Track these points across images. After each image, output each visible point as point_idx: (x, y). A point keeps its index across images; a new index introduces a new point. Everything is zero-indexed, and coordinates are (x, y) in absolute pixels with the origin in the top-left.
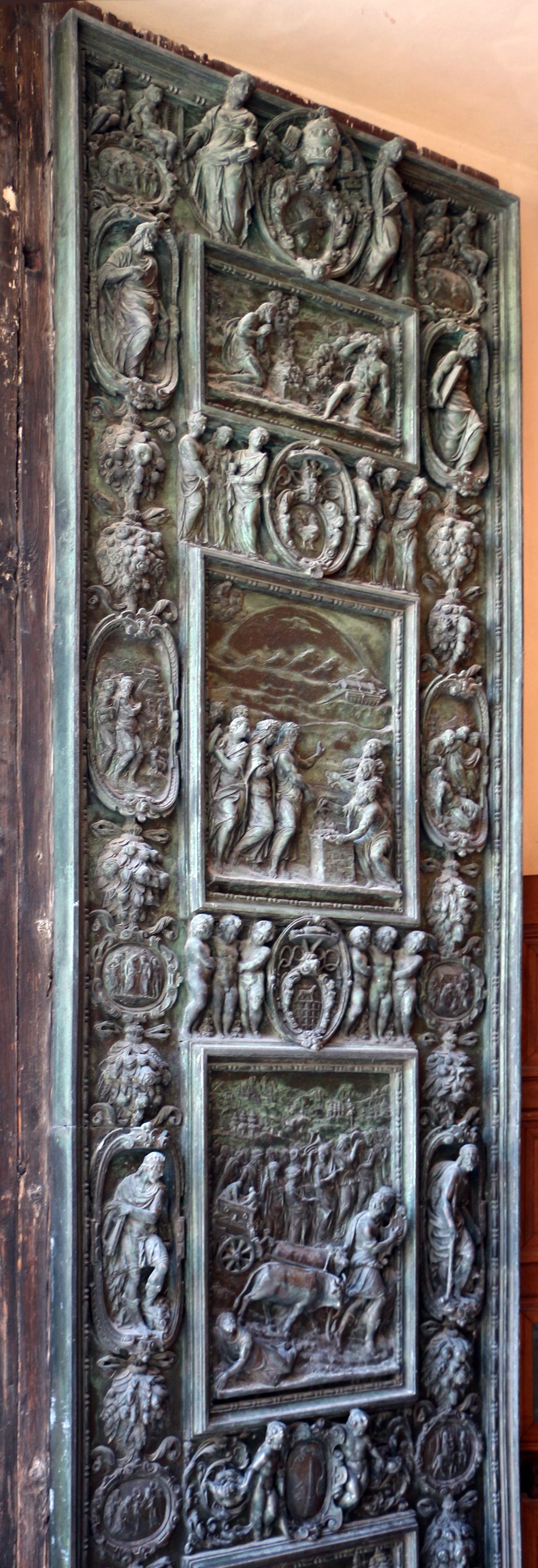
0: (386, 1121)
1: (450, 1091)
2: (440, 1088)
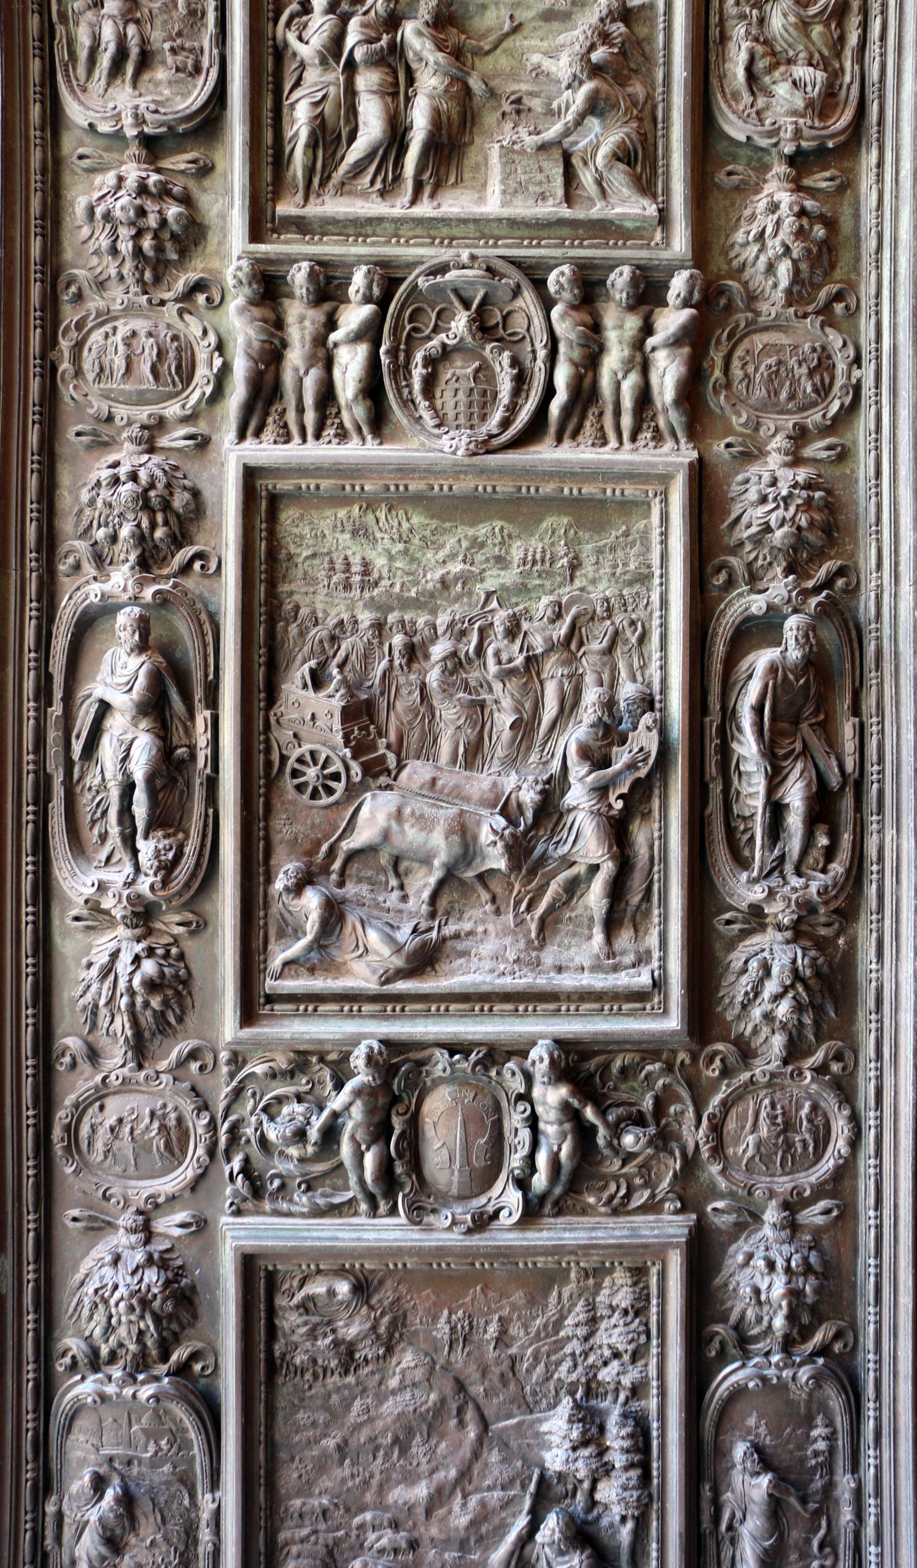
0: (643, 578)
1: (767, 529)
2: (749, 526)
